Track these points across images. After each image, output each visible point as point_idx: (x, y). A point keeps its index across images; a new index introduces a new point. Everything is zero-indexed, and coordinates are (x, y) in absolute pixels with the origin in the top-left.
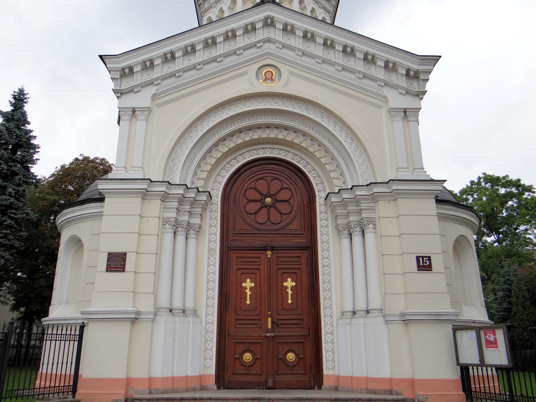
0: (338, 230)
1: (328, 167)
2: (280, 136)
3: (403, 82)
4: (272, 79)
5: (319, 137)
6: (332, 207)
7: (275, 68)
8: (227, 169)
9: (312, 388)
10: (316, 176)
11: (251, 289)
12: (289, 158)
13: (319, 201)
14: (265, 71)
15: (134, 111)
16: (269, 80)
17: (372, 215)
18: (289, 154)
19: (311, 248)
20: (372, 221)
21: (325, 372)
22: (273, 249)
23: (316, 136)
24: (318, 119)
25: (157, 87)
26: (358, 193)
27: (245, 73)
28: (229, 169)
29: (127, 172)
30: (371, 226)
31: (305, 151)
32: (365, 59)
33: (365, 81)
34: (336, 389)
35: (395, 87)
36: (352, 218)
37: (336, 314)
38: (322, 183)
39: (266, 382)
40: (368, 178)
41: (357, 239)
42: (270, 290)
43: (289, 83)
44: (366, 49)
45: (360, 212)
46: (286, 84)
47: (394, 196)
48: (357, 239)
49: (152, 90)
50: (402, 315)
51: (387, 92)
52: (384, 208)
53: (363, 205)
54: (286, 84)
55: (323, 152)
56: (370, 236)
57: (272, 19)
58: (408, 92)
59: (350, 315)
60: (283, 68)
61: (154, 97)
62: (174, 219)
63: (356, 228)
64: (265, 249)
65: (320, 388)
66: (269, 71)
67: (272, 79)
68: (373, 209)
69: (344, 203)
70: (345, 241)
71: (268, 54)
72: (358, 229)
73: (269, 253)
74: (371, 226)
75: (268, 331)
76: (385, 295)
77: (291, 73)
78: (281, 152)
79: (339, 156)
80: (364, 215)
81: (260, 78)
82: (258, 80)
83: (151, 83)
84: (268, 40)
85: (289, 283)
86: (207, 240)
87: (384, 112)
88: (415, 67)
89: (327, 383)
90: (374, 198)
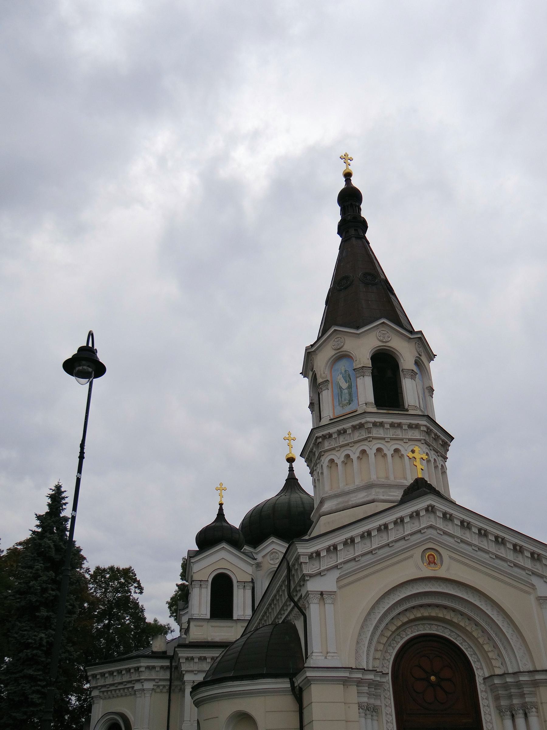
0: (500, 710)
1: (486, 647)
2: (441, 615)
4: (435, 563)
5: (478, 619)
6: (493, 688)
7: (435, 552)
8: (392, 645)
10: (472, 653)
12: (446, 634)
13: (479, 680)
14: (428, 554)
15: (322, 594)
16: (432, 563)
17: (534, 700)
18: (446, 631)
20: (535, 705)
24: (477, 603)
25: (339, 571)
26: (521, 678)
27: (411, 557)
28: (395, 645)
29: (326, 658)
30: (534, 710)
33: (516, 569)
36: (515, 701)
38: (479, 661)
40: (526, 663)
41: (520, 721)
43: (451, 569)
46: (448, 569)
48: (520, 721)
49: (336, 574)
51: (535, 580)
54: (448, 569)
55: (480, 631)
56: (533, 720)
57: (433, 507)
61: (338, 580)
62: (366, 704)
66: (431, 555)
67: (435, 563)
68: (533, 694)
69: (506, 686)
70: (508, 723)
71: (430, 538)
72: (521, 711)
74: (534, 710)
78: (439, 628)
79: (497, 639)
80: (527, 700)
81: (425, 562)
82: (423, 564)
83: (336, 567)
84: (431, 527)
86: (385, 722)
87: (532, 598)
90: (535, 684)
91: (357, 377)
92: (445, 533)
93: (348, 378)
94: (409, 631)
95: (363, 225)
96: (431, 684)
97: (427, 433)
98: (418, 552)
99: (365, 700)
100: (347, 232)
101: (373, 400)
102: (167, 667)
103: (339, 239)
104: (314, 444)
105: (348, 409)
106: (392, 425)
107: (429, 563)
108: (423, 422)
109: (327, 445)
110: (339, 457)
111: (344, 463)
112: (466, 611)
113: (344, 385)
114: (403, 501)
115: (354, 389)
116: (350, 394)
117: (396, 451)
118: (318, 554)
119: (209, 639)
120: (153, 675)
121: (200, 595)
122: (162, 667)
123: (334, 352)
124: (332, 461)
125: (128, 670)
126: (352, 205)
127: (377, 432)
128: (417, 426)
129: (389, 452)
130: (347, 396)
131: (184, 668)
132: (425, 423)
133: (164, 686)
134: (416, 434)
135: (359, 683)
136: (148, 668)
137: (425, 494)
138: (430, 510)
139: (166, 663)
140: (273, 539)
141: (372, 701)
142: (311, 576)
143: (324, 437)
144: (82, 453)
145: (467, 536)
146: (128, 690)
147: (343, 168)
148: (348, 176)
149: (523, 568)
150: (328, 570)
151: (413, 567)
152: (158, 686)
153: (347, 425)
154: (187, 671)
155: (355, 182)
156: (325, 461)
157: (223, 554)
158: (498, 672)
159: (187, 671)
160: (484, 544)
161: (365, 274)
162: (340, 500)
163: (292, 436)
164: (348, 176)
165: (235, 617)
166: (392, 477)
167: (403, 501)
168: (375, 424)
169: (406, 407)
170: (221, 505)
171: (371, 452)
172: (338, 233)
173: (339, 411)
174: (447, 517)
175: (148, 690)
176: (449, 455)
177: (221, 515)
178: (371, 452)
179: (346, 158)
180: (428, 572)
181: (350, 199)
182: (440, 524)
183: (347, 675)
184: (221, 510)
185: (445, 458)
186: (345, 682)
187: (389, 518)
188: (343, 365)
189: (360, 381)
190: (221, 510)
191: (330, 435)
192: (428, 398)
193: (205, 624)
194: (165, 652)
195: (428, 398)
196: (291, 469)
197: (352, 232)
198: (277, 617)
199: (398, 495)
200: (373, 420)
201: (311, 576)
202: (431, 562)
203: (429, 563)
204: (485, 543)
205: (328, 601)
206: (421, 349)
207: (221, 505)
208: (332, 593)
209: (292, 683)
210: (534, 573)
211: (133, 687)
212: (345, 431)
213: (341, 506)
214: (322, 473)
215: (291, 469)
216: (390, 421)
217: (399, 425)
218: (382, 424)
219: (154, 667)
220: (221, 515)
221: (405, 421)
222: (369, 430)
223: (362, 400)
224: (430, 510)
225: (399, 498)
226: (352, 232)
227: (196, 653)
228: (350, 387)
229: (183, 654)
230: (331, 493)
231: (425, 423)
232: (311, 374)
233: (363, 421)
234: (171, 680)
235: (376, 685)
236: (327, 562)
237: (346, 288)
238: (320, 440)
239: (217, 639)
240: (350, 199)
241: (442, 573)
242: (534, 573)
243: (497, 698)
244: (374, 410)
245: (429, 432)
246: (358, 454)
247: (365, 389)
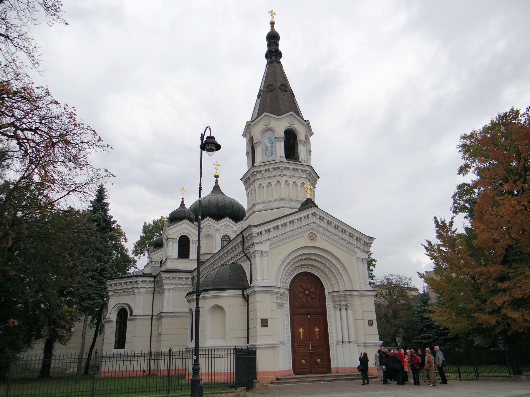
0: (335, 307)
3: (362, 247)
6: (333, 297)
9: (327, 373)
11: (303, 332)
12: (314, 272)
13: (326, 293)
15: (262, 252)
17: (351, 303)
19: (324, 315)
20: (351, 305)
21: (332, 366)
22: (310, 315)
23: (327, 264)
26: (347, 293)
31: (324, 273)
32: (350, 236)
34: (337, 373)
35: (359, 248)
36: (343, 303)
37: (335, 343)
39: (311, 371)
42: (309, 332)
43: (320, 243)
44: (351, 232)
45: (346, 300)
47: (360, 296)
48: (344, 311)
49: (269, 243)
50: (364, 343)
51: (357, 250)
52: (356, 300)
53: (348, 298)
56: (350, 311)
57: (315, 213)
58: (364, 251)
59: (341, 343)
61: (270, 246)
63: (343, 306)
64: (307, 315)
65: (330, 373)
68: (351, 300)
69: (339, 296)
73: (309, 316)
75: (310, 350)
76: (357, 336)
77: (321, 237)
84: (313, 223)
85: (317, 330)
87: (355, 258)
88: (367, 241)
89: (333, 370)
90: (352, 296)
91: (276, 142)
92: (320, 226)
93: (271, 142)
94: (297, 270)
95: (279, 55)
96: (306, 295)
97: (310, 175)
99: (279, 301)
100: (271, 58)
101: (284, 155)
102: (153, 281)
103: (266, 61)
104: (251, 175)
105: (270, 158)
106: (293, 169)
107: (311, 239)
108: (308, 169)
109: (258, 176)
110: (265, 183)
111: (267, 186)
113: (269, 145)
114: (301, 210)
115: (274, 148)
116: (272, 150)
117: (294, 182)
118: (261, 233)
119: (177, 268)
120: (145, 285)
121: (173, 245)
122: (150, 281)
123: (264, 127)
124: (261, 185)
125: (131, 282)
126: (274, 42)
127: (286, 172)
128: (305, 171)
129: (291, 183)
130: (270, 152)
131: (164, 282)
132: (309, 169)
133: (151, 291)
134: (304, 175)
135: (277, 293)
136: (142, 281)
137: (311, 207)
138: (314, 214)
139: (152, 279)
140: (208, 218)
141: (281, 302)
142: (257, 243)
143: (257, 172)
144: (200, 187)
145: (330, 228)
146: (131, 292)
147: (270, 19)
148: (272, 24)
149: (352, 244)
150: (265, 240)
151: (304, 241)
152: (148, 291)
153: (271, 167)
155: (277, 29)
156: (257, 184)
157: (185, 225)
158: (336, 290)
160: (336, 232)
161: (282, 85)
162: (265, 205)
163: (218, 164)
164: (272, 24)
165: (191, 258)
166: (292, 196)
167: (301, 210)
168: (285, 168)
169: (300, 160)
170: (183, 199)
171: (282, 182)
172: (266, 57)
173: (265, 159)
174: (321, 219)
175: (142, 292)
176: (316, 186)
177: (182, 204)
178: (282, 182)
179: (272, 13)
181: (273, 38)
182: (318, 221)
183: (273, 290)
184: (183, 202)
185: (315, 187)
186: (271, 293)
187: (295, 217)
188: (268, 134)
189: (278, 144)
190: (183, 202)
191: (261, 171)
192: (309, 156)
194: (151, 274)
195: (309, 156)
196: (217, 182)
197: (274, 58)
198: (229, 261)
199: (299, 206)
200: (284, 166)
201: (257, 243)
202: (312, 239)
203: (311, 239)
204: (337, 232)
205: (264, 255)
206: (308, 130)
207: (183, 199)
208: (267, 252)
209: (243, 292)
210: (357, 247)
211: (133, 291)
212: (269, 170)
213: (265, 208)
214: (255, 190)
215: (217, 182)
216: (293, 167)
217: (297, 170)
218: (288, 168)
219: (145, 281)
220: (182, 204)
221: (300, 168)
222: (282, 171)
223: (279, 155)
224: (314, 214)
225: (299, 207)
226: (274, 58)
227: (171, 275)
228: (272, 147)
229: (164, 275)
230: (259, 201)
231: (309, 169)
232: (248, 136)
233: (279, 166)
234: (154, 288)
235: (283, 294)
236: (265, 237)
237: (271, 91)
238: (255, 173)
240: (273, 38)
241: (316, 245)
242: (357, 247)
243: (334, 301)
244: (285, 160)
245: (310, 174)
246: (275, 182)
247: (280, 148)
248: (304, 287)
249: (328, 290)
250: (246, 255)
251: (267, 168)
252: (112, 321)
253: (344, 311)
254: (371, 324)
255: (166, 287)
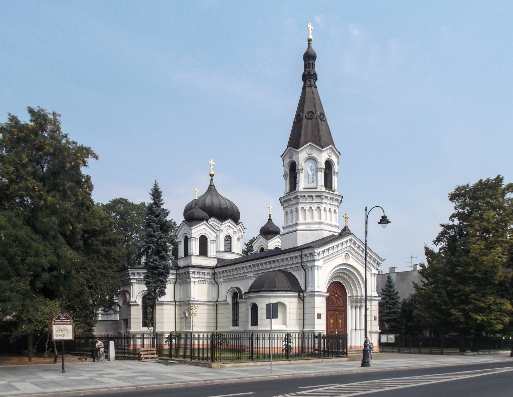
0: (352, 306)
13: (348, 297)
19: (345, 311)
42: (336, 323)
48: (358, 310)
51: (372, 268)
60: (350, 255)
85: (340, 321)
98: (344, 254)
112: (349, 274)
131: (191, 275)
154: (193, 277)
158: (354, 295)
159: (193, 277)
180: (345, 262)
193: (197, 257)
213: (308, 229)
222: (322, 199)
227: (196, 270)
239: (203, 264)
248: (335, 291)
249: (348, 295)
250: (302, 266)
251: (310, 194)
252: (138, 305)
253: (358, 310)
254: (375, 319)
255: (192, 279)
